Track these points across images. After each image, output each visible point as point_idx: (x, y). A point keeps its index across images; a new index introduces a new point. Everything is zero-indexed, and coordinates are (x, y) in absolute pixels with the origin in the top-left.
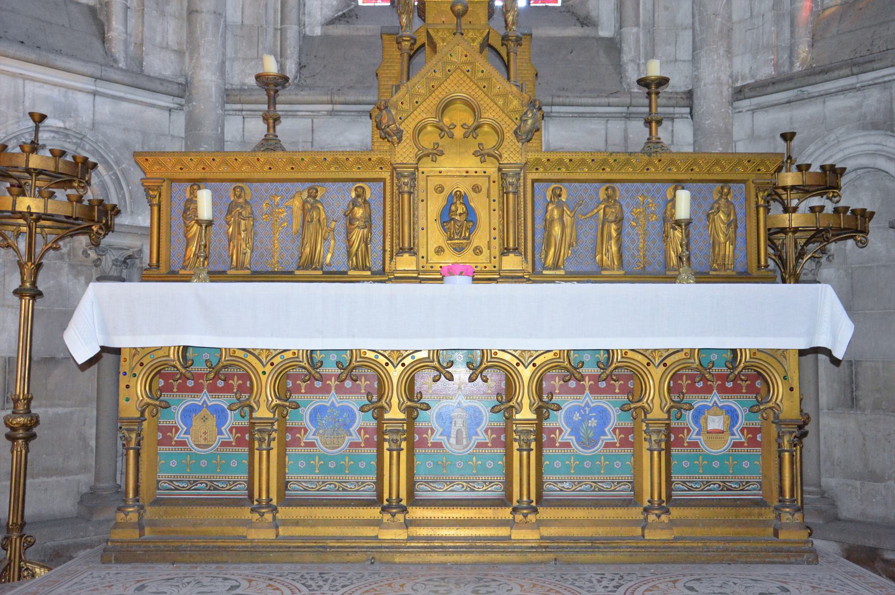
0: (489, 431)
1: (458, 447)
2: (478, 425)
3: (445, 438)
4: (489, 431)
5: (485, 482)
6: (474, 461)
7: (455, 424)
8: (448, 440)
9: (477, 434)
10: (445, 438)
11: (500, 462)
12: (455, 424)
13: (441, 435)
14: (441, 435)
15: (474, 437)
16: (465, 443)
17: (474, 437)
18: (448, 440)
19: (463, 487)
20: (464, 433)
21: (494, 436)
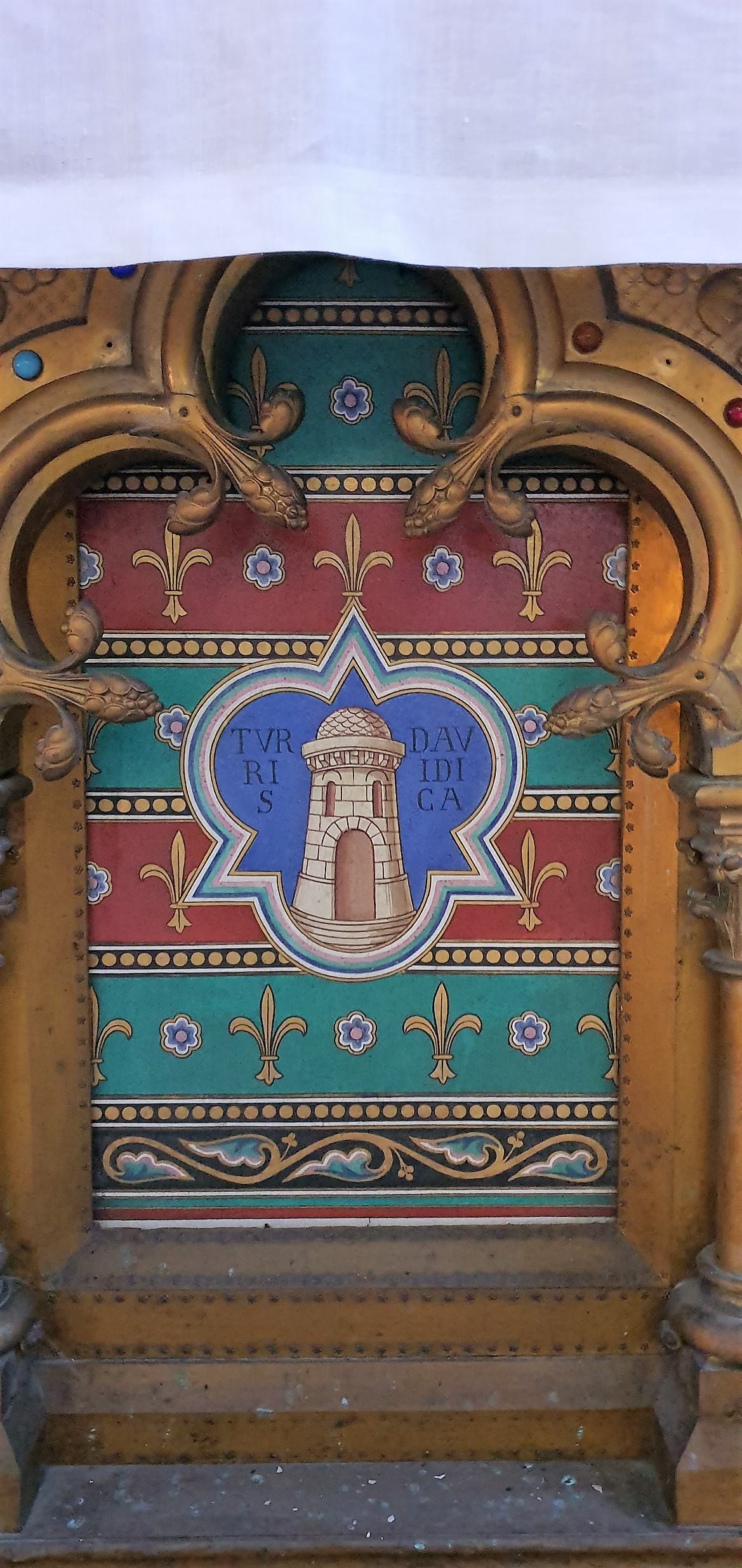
0: (529, 844)
1: (342, 933)
2: (464, 808)
3: (271, 882)
4: (529, 844)
5: (502, 1135)
6: (440, 1012)
7: (328, 800)
8: (289, 896)
9: (456, 861)
10: (271, 882)
11: (592, 1022)
12: (328, 800)
13: (246, 864)
14: (246, 864)
15: (437, 879)
16: (385, 909)
17: (437, 879)
18: (289, 896)
19: (377, 1156)
20: (382, 853)
21: (556, 869)
